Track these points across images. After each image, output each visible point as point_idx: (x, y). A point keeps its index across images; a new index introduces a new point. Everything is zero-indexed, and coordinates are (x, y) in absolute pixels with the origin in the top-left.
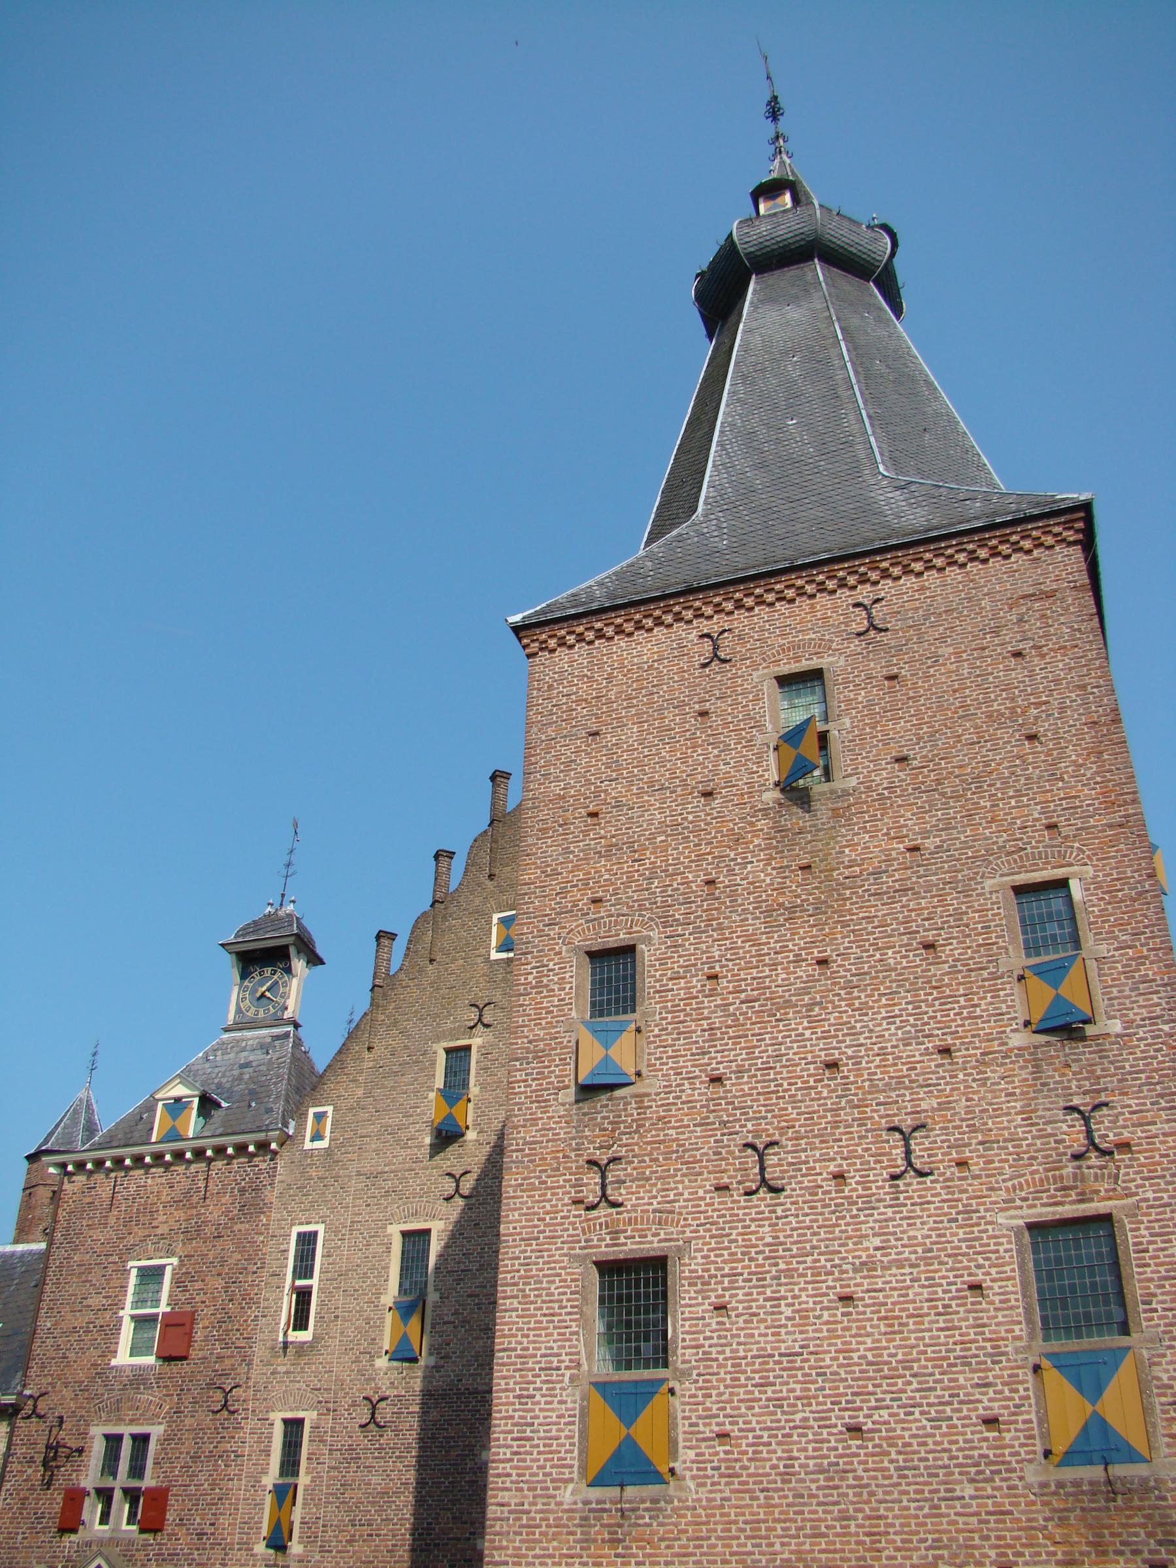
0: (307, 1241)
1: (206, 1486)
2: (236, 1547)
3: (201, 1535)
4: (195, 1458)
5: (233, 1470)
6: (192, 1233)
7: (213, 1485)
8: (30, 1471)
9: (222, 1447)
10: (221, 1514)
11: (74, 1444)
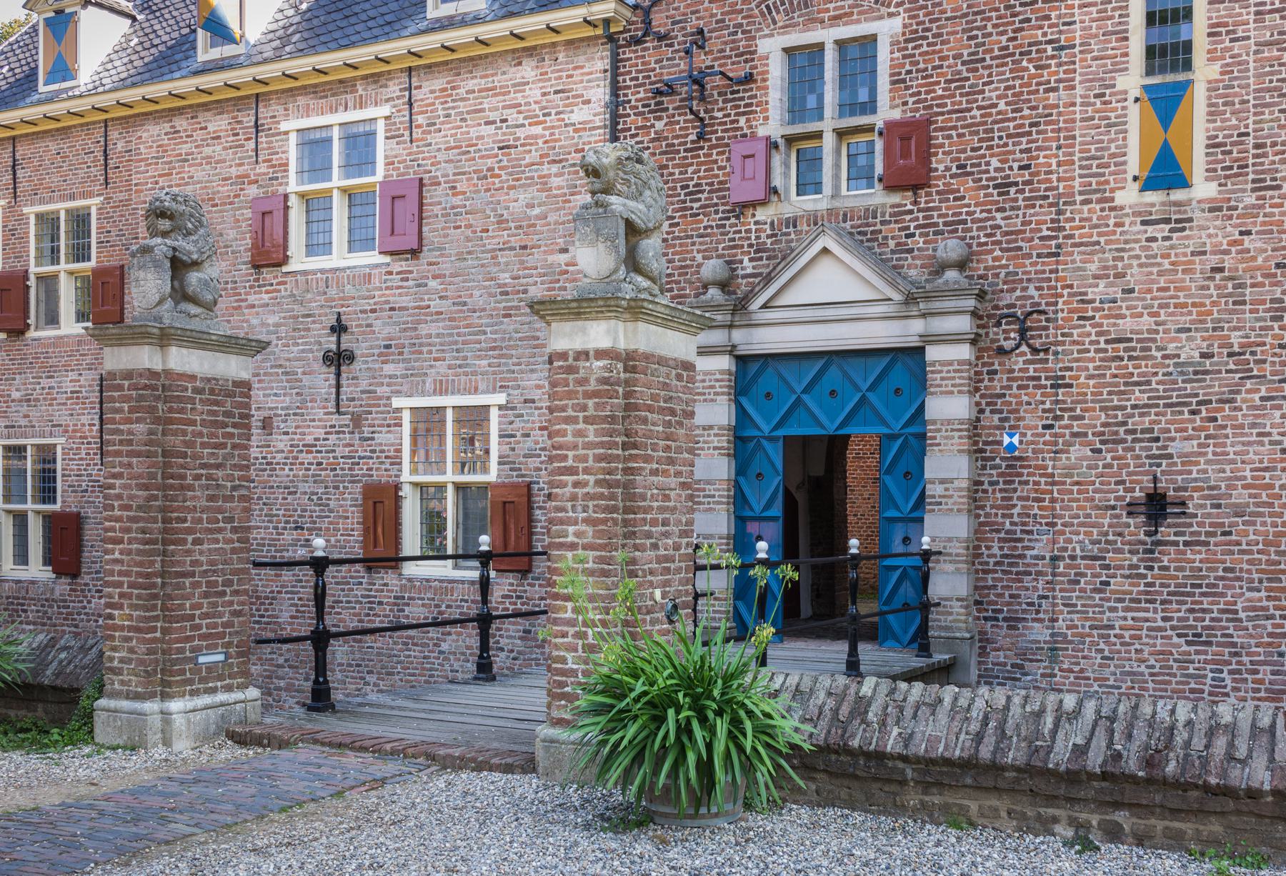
1: (1002, 106)
2: (1079, 198)
3: (1003, 187)
4: (974, 63)
5: (1053, 72)
8: (659, 125)
9: (1025, 38)
10: (1038, 149)
11: (738, 72)
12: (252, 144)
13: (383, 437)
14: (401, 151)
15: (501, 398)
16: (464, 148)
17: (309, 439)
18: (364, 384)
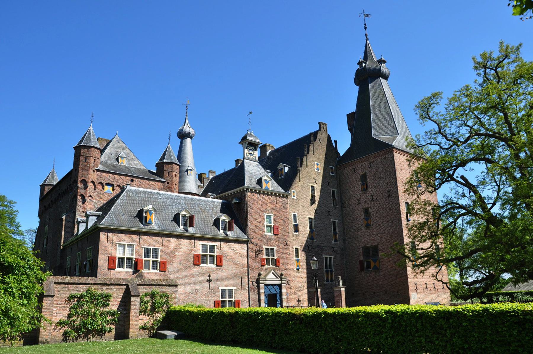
0: (295, 216)
6: (275, 210)
7: (286, 258)
8: (253, 254)
12: (193, 244)
13: (217, 293)
14: (219, 251)
15: (235, 288)
16: (228, 252)
17: (204, 293)
18: (213, 285)
